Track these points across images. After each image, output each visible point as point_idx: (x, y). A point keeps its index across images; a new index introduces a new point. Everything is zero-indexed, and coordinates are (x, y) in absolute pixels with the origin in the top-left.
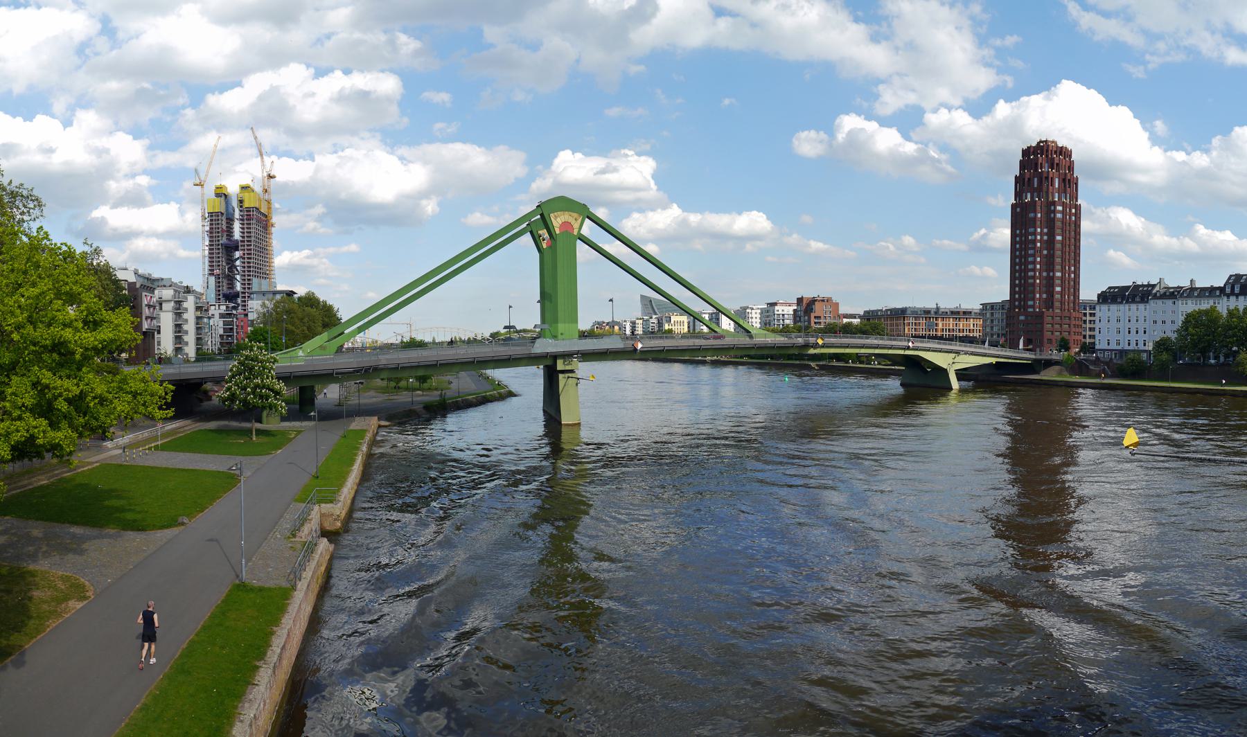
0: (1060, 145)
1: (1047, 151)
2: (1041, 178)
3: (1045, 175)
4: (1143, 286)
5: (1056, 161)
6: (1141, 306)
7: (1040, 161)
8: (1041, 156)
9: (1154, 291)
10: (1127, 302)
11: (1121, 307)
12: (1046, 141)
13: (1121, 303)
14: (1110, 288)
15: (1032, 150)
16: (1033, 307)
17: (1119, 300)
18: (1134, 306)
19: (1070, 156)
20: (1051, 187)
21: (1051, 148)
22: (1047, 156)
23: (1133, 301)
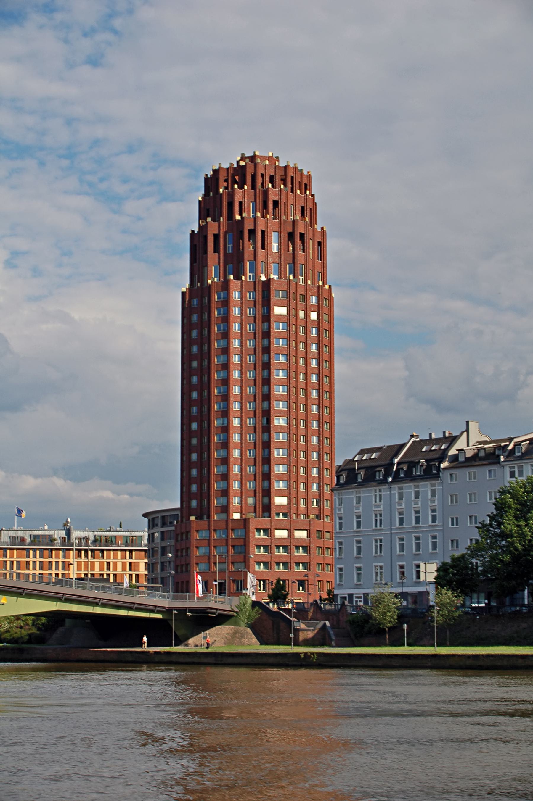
0: (282, 163)
1: (254, 177)
2: (242, 233)
3: (248, 226)
4: (431, 441)
5: (273, 196)
6: (425, 487)
7: (237, 199)
8: (241, 187)
9: (453, 452)
10: (397, 479)
11: (385, 491)
12: (253, 158)
13: (384, 482)
14: (363, 452)
15: (222, 177)
16: (225, 509)
17: (379, 476)
18: (409, 489)
19: (307, 187)
20: (260, 251)
21: (260, 171)
22: (254, 187)
23: (409, 477)
